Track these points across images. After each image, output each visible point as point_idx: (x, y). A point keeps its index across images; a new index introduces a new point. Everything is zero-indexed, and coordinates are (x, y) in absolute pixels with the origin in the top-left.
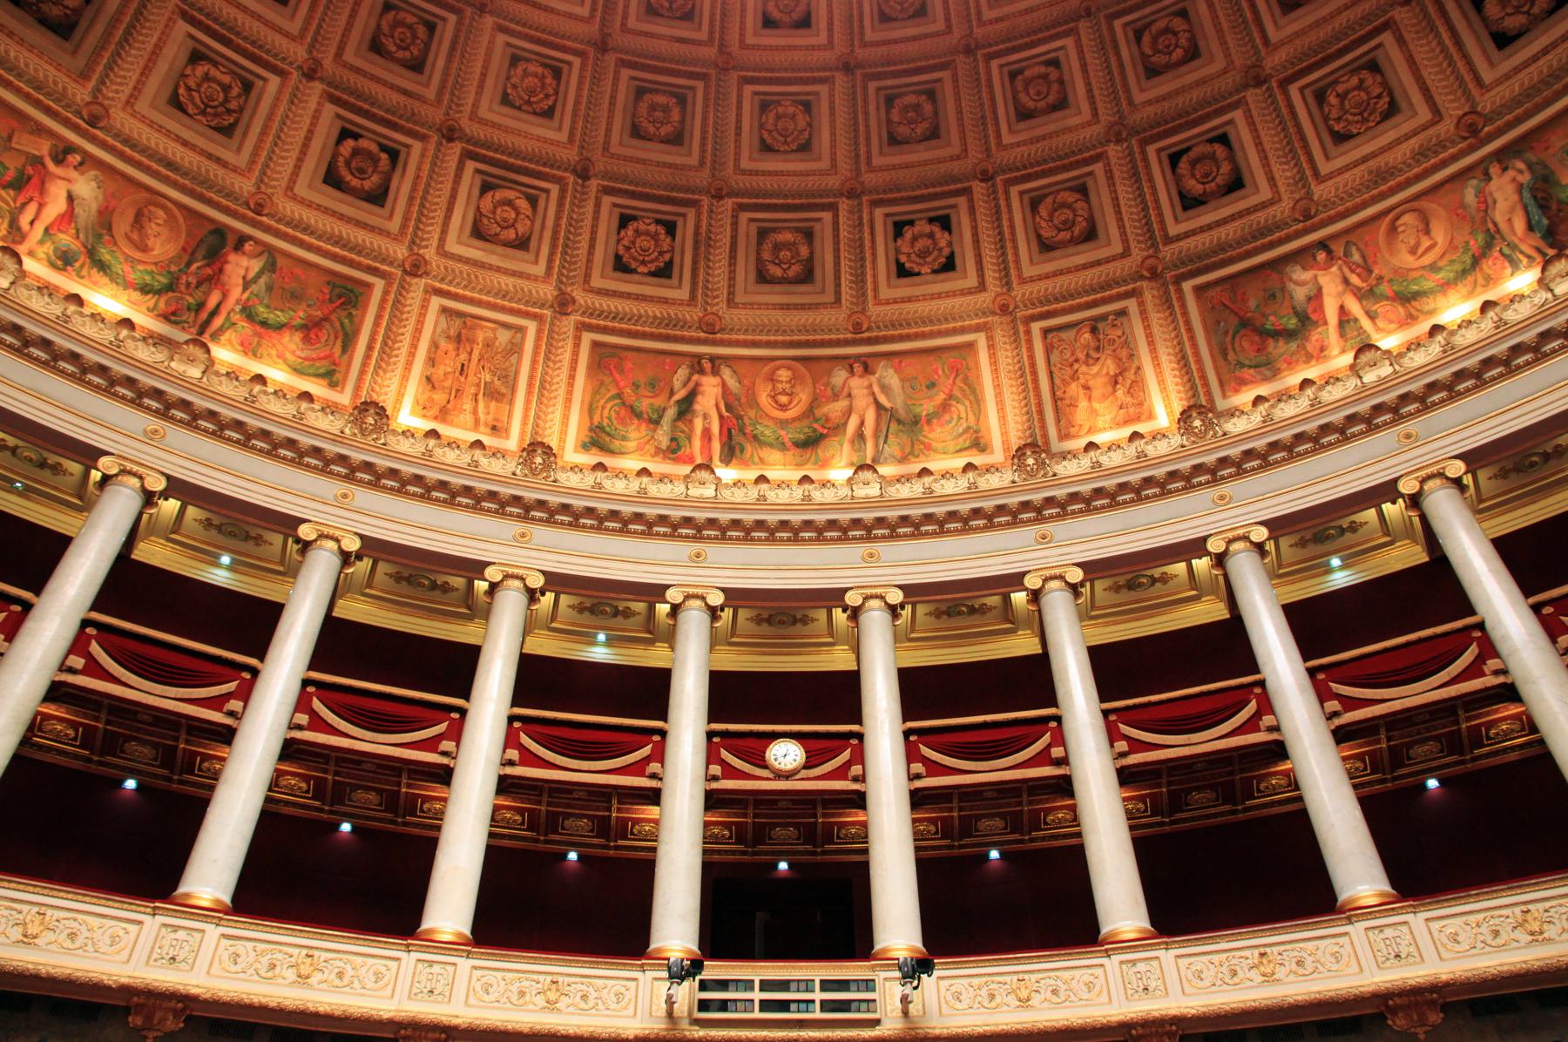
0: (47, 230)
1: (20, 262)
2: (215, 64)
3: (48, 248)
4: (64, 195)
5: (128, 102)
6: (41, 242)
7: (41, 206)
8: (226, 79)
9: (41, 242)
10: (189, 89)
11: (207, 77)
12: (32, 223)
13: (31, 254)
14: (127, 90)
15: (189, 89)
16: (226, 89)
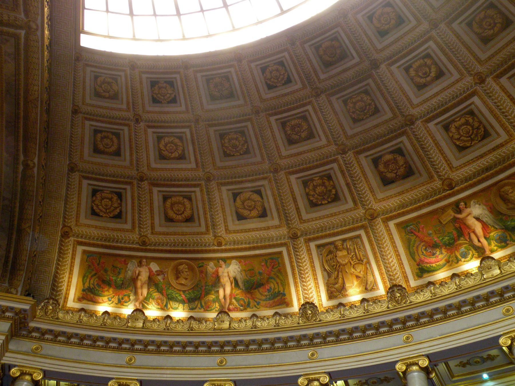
0: (485, 238)
1: (493, 258)
2: (454, 121)
3: (493, 244)
4: (474, 220)
5: (450, 168)
6: (489, 244)
7: (474, 232)
8: (463, 120)
9: (489, 244)
10: (458, 139)
11: (458, 129)
12: (479, 241)
13: (492, 251)
14: (445, 165)
15: (458, 139)
16: (467, 123)
